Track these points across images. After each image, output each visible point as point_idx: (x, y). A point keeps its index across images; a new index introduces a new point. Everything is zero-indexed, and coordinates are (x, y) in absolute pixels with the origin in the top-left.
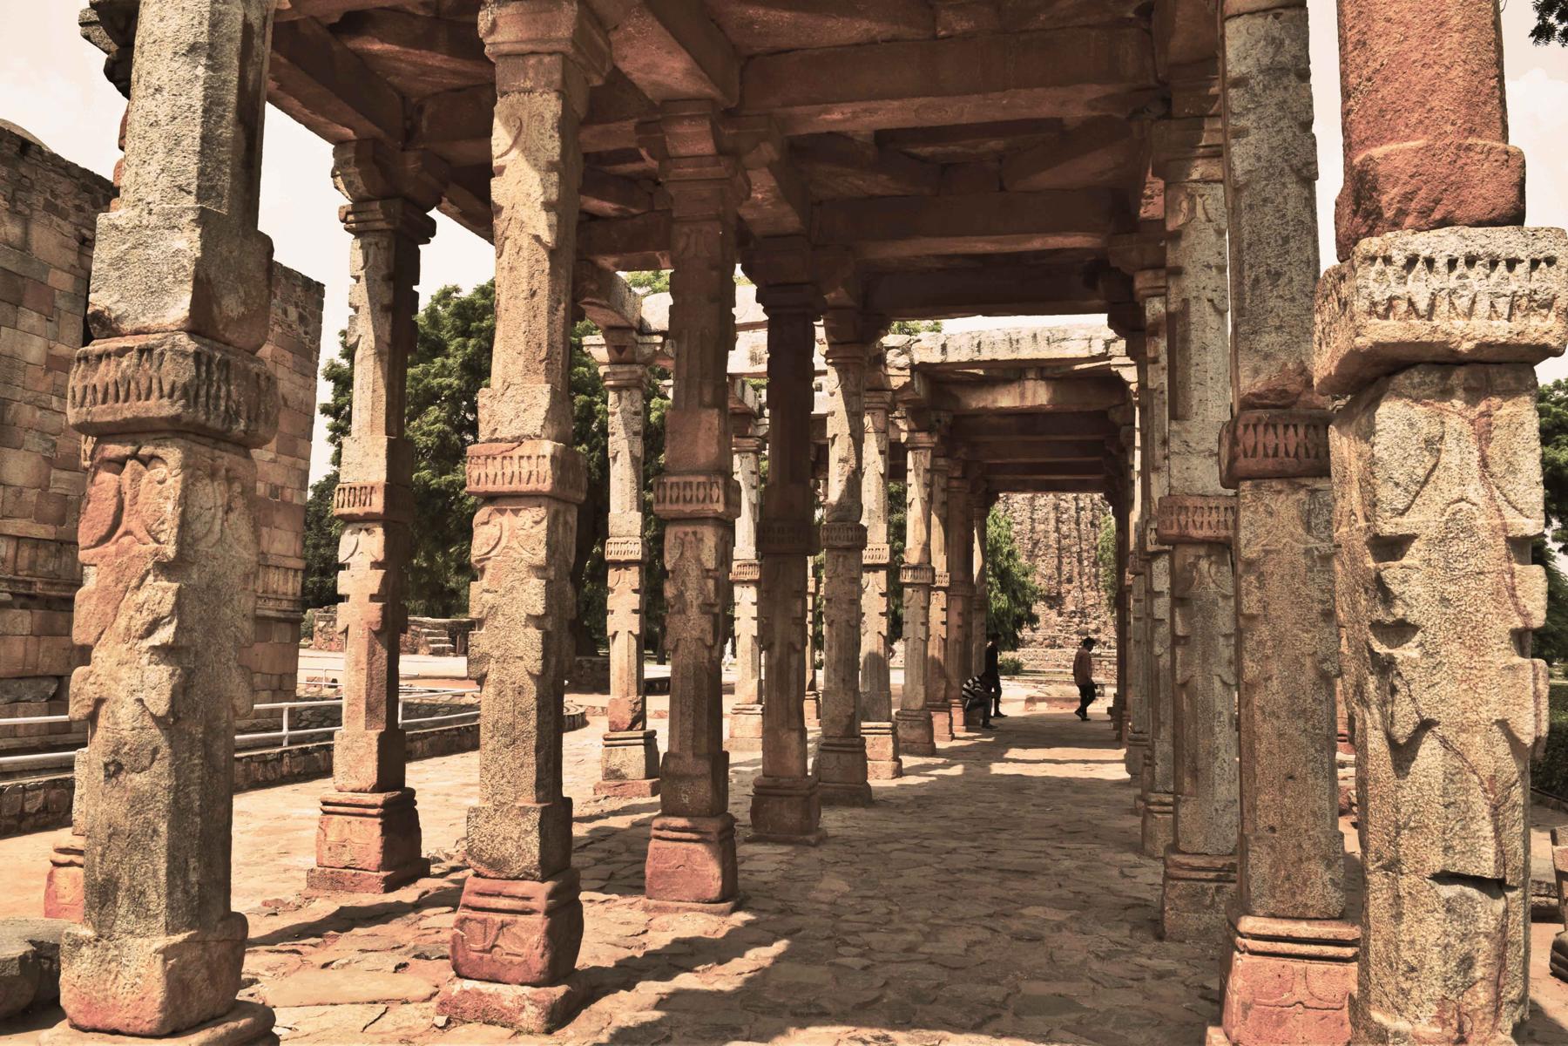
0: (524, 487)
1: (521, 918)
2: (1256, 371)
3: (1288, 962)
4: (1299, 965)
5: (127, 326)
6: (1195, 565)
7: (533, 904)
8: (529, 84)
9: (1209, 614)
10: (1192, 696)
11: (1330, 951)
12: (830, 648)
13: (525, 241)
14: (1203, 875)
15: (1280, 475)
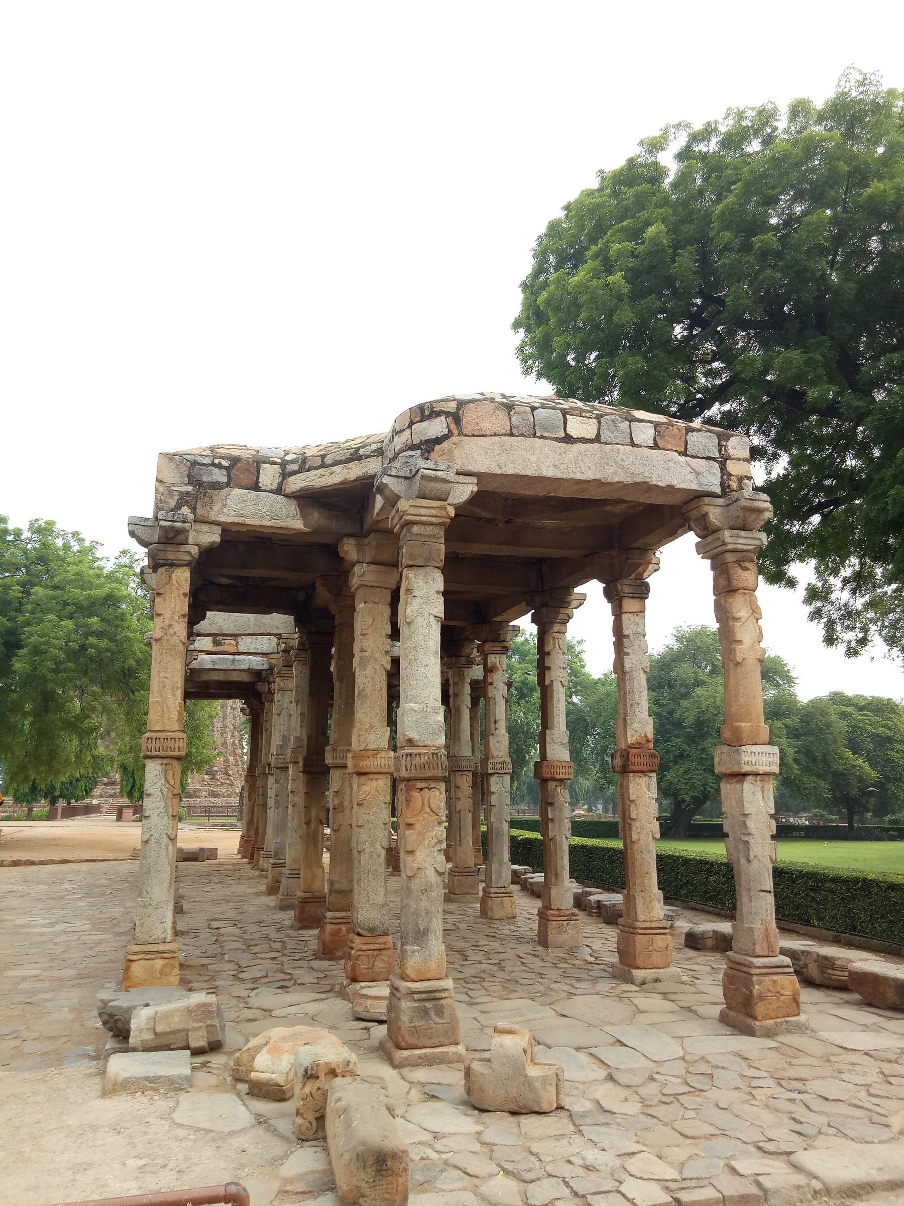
0: (382, 771)
1: (384, 952)
2: (633, 736)
3: (650, 936)
4: (654, 937)
5: (420, 744)
6: (555, 789)
7: (388, 945)
8: (377, 600)
9: (561, 810)
10: (555, 845)
11: (662, 931)
12: (293, 819)
13: (377, 667)
14: (562, 918)
15: (642, 772)
